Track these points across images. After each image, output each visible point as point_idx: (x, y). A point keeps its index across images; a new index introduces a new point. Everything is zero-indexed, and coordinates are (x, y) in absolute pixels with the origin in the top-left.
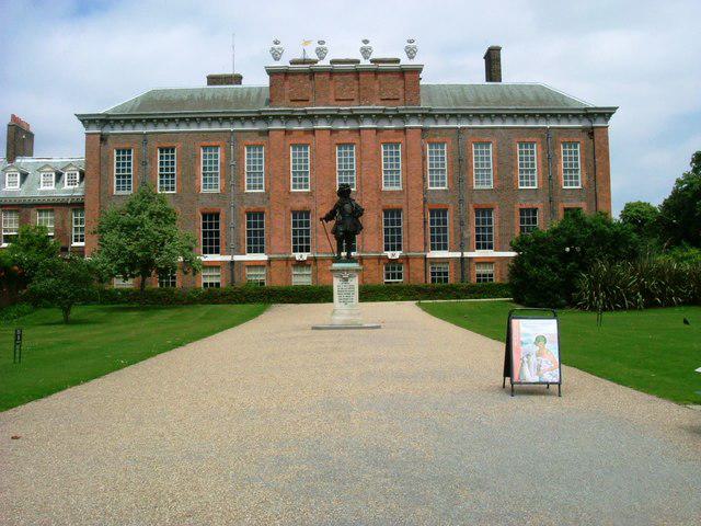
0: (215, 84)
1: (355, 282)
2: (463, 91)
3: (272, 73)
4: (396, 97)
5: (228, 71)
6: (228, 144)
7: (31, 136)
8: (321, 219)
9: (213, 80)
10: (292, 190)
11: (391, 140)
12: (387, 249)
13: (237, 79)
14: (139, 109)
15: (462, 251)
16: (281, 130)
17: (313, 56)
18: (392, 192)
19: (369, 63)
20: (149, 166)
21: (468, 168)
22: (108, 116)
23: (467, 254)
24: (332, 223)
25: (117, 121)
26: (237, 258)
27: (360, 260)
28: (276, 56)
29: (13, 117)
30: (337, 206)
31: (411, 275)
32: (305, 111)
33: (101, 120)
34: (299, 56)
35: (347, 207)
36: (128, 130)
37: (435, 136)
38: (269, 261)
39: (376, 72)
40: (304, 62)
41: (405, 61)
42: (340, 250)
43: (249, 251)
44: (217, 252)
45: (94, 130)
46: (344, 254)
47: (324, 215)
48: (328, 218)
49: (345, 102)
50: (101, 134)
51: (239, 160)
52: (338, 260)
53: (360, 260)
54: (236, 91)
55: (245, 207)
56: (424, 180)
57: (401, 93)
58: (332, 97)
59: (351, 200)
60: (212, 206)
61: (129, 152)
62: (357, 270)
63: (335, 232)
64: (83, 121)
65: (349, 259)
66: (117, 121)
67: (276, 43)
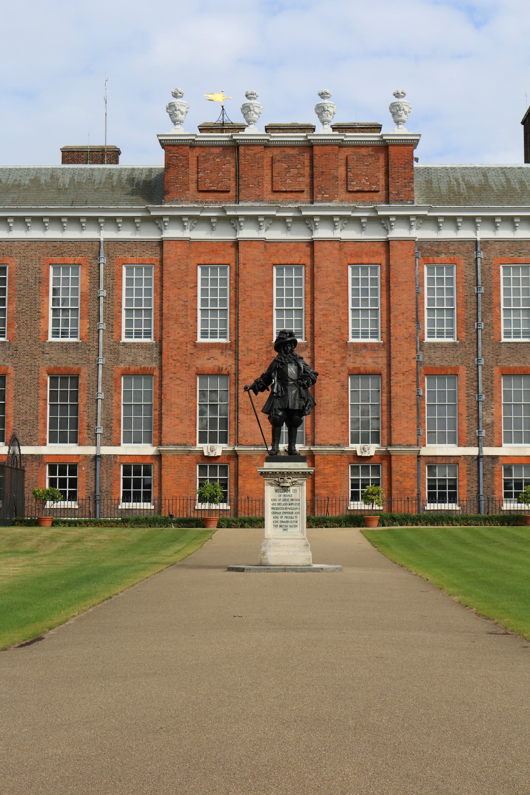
0: (74, 161)
1: (300, 493)
2: (485, 175)
3: (168, 145)
4: (374, 187)
5: (96, 141)
6: (95, 262)
8: (246, 389)
9: (70, 155)
10: (200, 340)
11: (366, 260)
12: (355, 440)
13: (112, 155)
15: (478, 442)
17: (238, 119)
18: (365, 345)
19: (330, 131)
21: (492, 306)
23: (488, 451)
24: (264, 395)
26: (106, 450)
27: (310, 458)
30: (271, 369)
31: (394, 484)
34: (214, 118)
35: (292, 370)
37: (438, 253)
38: (159, 457)
39: (341, 145)
40: (222, 127)
41: (391, 130)
42: (276, 438)
43: (127, 440)
44: (75, 440)
46: (283, 446)
47: (251, 382)
48: (259, 386)
49: (289, 195)
51: (114, 287)
52: (273, 456)
53: (310, 458)
54: (110, 175)
55: (122, 366)
56: (418, 321)
57: (382, 182)
58: (269, 187)
59: (296, 360)
60: (67, 361)
62: (304, 474)
63: (268, 410)
65: (292, 455)
67: (175, 95)
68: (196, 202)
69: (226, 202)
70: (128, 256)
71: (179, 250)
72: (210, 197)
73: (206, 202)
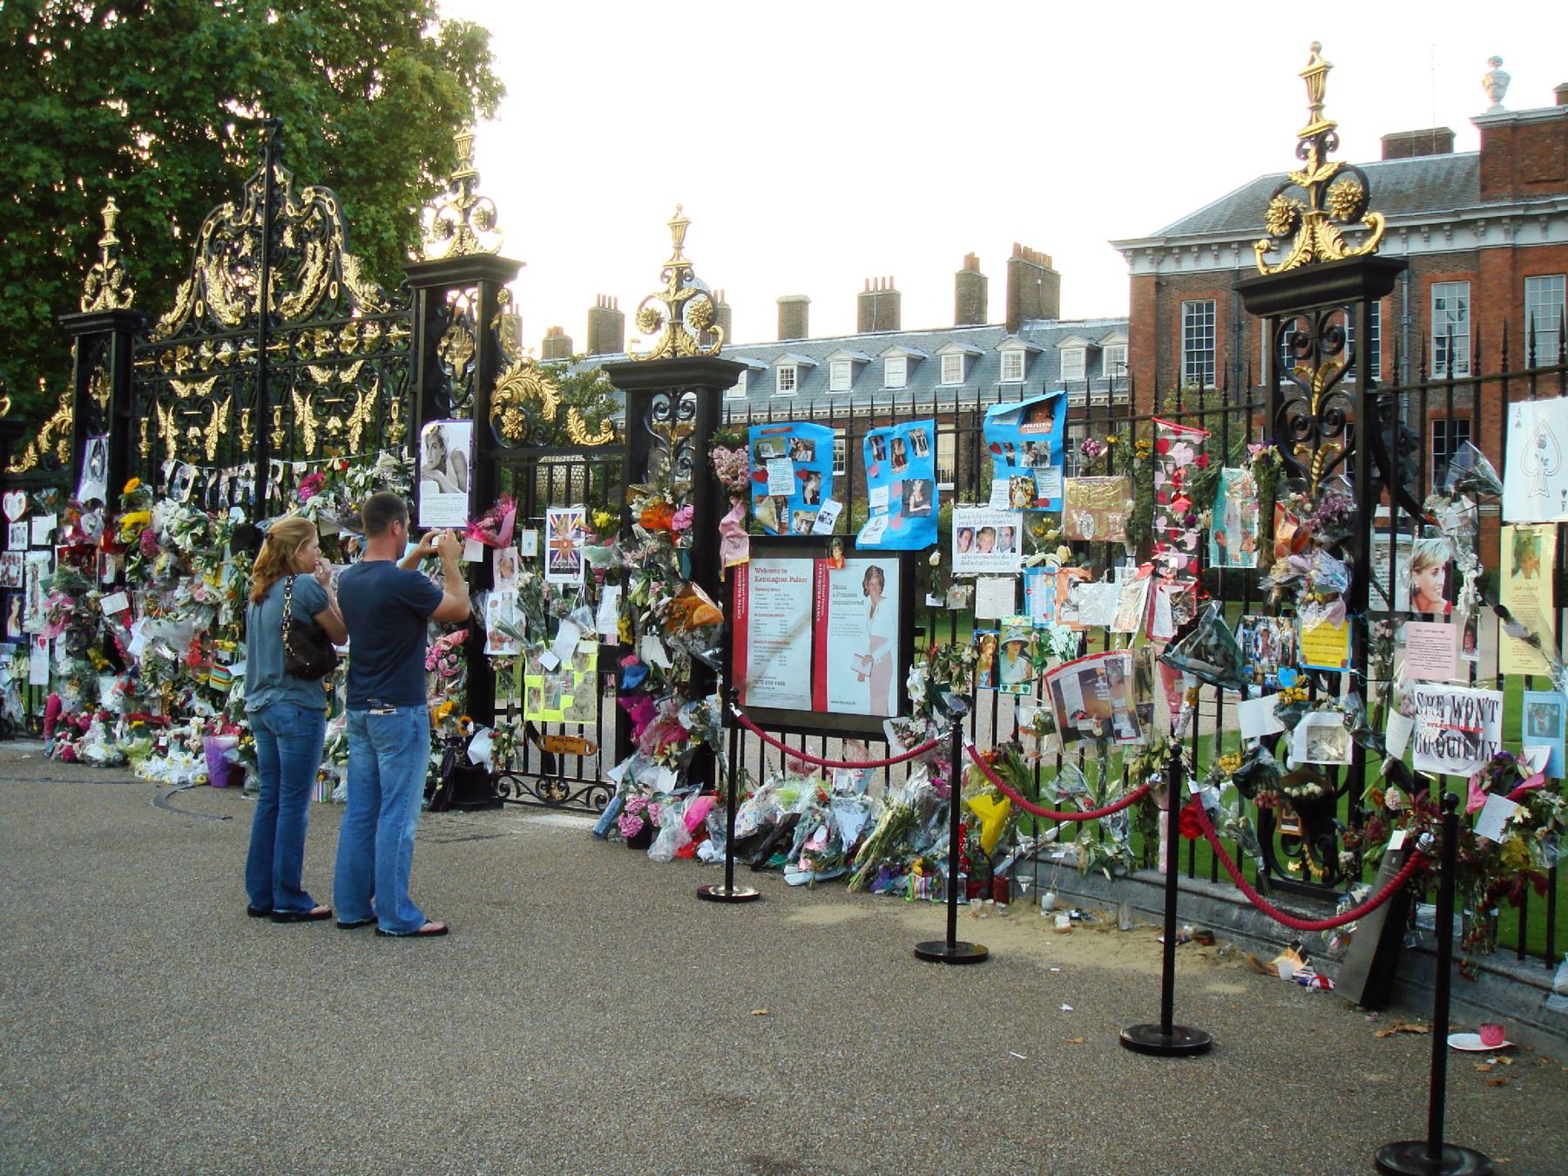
7: (1052, 279)
14: (1228, 223)
16: (1502, 248)
20: (1245, 334)
22: (1169, 240)
25: (1185, 249)
28: (1498, 85)
29: (1017, 247)
32: (1553, 204)
33: (1156, 249)
36: (1208, 264)
45: (1145, 267)
50: (1158, 276)
61: (1210, 307)
64: (1124, 251)
66: (1185, 249)
68: (1521, 197)
69: (1554, 195)
70: (1437, 272)
71: (1499, 260)
72: (1540, 190)
73: (1535, 197)
